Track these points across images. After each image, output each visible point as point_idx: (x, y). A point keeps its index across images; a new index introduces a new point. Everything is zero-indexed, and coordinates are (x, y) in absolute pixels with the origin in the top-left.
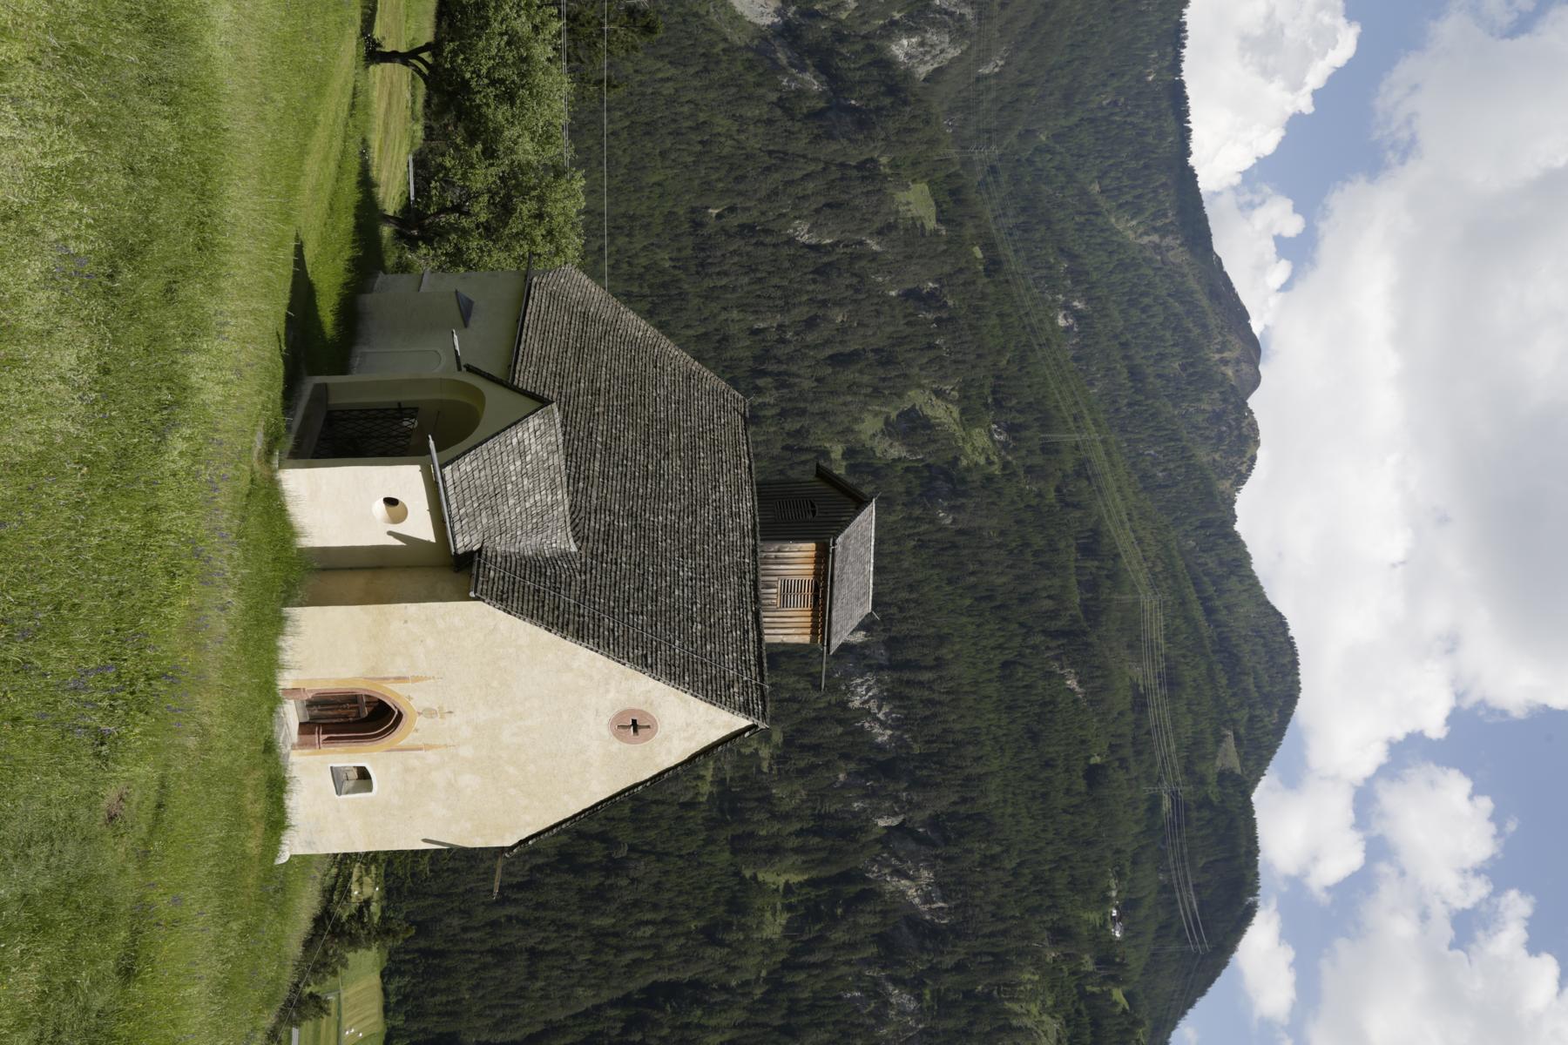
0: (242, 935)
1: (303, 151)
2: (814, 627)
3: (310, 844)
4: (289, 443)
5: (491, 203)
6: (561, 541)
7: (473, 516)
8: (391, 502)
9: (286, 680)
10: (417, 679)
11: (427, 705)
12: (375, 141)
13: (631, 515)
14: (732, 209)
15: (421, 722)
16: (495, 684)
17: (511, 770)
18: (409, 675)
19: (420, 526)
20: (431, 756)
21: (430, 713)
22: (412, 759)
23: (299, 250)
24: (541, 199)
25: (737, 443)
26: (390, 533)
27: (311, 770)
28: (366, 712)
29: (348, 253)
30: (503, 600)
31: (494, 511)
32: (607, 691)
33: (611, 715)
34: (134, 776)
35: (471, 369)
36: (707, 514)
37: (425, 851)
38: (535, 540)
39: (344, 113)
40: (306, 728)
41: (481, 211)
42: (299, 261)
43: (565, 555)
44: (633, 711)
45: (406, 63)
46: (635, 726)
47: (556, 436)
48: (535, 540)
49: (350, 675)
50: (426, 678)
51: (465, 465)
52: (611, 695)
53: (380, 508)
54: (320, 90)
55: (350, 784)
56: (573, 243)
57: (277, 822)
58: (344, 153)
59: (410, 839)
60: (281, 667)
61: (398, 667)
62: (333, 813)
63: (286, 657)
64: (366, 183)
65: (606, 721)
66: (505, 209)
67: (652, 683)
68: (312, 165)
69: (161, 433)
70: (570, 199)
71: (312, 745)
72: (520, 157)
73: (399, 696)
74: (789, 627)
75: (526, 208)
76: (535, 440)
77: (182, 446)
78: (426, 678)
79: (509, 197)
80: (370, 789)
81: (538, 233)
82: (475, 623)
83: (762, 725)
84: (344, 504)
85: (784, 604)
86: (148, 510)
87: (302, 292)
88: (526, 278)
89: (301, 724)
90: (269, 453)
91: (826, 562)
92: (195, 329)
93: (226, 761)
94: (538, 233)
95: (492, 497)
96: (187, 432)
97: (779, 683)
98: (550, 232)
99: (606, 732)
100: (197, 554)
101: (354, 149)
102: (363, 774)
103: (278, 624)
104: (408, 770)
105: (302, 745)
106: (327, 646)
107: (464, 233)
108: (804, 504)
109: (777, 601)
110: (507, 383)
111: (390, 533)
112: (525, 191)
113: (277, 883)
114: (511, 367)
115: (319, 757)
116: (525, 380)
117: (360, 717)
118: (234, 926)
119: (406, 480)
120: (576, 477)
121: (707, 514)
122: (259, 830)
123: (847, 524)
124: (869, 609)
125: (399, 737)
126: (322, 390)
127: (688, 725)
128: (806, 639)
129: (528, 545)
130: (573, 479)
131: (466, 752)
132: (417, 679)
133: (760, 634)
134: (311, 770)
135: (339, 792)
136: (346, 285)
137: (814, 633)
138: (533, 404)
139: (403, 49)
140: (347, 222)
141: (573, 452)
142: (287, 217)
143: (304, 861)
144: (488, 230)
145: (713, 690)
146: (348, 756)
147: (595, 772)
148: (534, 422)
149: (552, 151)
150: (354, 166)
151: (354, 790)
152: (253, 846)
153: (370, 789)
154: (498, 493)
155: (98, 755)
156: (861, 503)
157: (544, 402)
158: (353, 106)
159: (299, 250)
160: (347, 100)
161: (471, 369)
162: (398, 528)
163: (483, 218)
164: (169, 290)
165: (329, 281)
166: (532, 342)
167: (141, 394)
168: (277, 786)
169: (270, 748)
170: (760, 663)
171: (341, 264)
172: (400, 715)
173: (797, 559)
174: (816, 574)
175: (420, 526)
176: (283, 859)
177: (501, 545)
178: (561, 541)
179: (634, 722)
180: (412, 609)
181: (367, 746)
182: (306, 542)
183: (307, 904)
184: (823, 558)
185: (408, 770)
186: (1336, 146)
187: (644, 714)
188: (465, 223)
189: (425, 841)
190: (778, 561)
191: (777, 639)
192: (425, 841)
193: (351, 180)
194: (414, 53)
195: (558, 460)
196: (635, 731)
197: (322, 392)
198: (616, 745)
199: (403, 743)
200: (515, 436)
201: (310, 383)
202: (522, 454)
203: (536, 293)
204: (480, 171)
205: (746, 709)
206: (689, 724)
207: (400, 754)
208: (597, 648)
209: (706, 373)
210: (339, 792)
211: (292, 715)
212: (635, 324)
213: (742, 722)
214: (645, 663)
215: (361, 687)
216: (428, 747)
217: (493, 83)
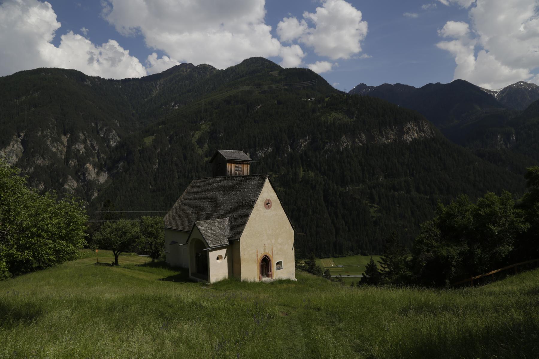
0: (312, 287)
1: (138, 279)
2: (246, 164)
3: (293, 274)
4: (204, 281)
5: (149, 237)
6: (226, 220)
7: (221, 240)
8: (218, 259)
9: (257, 280)
10: (257, 252)
12: (135, 263)
13: (220, 205)
14: (150, 183)
15: (267, 251)
17: (277, 231)
19: (223, 252)
20: (274, 249)
21: (265, 249)
22: (275, 253)
23: (160, 280)
24: (148, 226)
25: (204, 181)
27: (277, 274)
28: (264, 263)
29: (161, 269)
30: (239, 233)
31: (220, 236)
34: (277, 310)
35: (187, 241)
36: (220, 188)
37: (295, 250)
38: (226, 226)
39: (130, 270)
40: (268, 276)
41: (151, 239)
42: (163, 280)
43: (229, 220)
45: (118, 256)
46: (268, 204)
47: (202, 222)
48: (226, 226)
51: (209, 242)
53: (219, 261)
54: (124, 275)
55: (280, 267)
56: (158, 219)
57: (288, 281)
58: (138, 270)
59: (292, 253)
60: (255, 281)
61: (255, 256)
62: (286, 270)
63: (252, 280)
64: (145, 265)
65: (267, 210)
66: (151, 234)
67: (258, 200)
68: (141, 277)
69: (202, 307)
70: (148, 219)
71: (272, 275)
72: (138, 231)
74: (246, 169)
75: (150, 229)
76: (203, 227)
77: (205, 303)
79: (148, 233)
80: (281, 262)
81: (156, 226)
82: (245, 240)
83: (268, 175)
84: (218, 268)
85: (241, 171)
86: (220, 310)
87: (170, 279)
88: (166, 229)
90: (207, 285)
92: (179, 300)
93: (275, 292)
94: (156, 226)
95: (217, 236)
96: (202, 302)
97: (259, 172)
98: (156, 224)
99: (269, 210)
100: (229, 300)
101: (137, 268)
102: (279, 263)
103: (245, 282)
104: (277, 254)
105: (272, 277)
106: (250, 272)
107: (156, 243)
108: (218, 166)
109: (240, 172)
110: (190, 233)
112: (146, 229)
113: (301, 280)
114: (186, 232)
116: (189, 229)
117: (265, 265)
118: (310, 289)
119: (213, 255)
120: (212, 217)
121: (220, 188)
122: (290, 285)
123: (223, 156)
124: (242, 151)
125: (270, 255)
126: (192, 274)
128: (249, 166)
129: (227, 228)
130: (212, 218)
131: (273, 241)
132: (257, 252)
133: (248, 176)
134: (277, 274)
136: (169, 269)
137: (247, 164)
138: (195, 227)
139: (114, 257)
140: (154, 269)
141: (206, 218)
142: (153, 282)
143: (297, 276)
144: (156, 238)
145: (260, 187)
146: (274, 267)
147: (278, 212)
148: (199, 227)
149: (137, 223)
150: (141, 268)
152: (293, 286)
153: (281, 262)
154: (215, 235)
155: (273, 318)
156: (218, 153)
157: (195, 225)
158: (128, 268)
159: (160, 280)
160: (126, 270)
161: (187, 241)
163: (153, 239)
164: (170, 306)
165: (167, 273)
166: (181, 228)
167: (193, 311)
168: (280, 282)
169: (272, 283)
170: (253, 176)
171: (164, 270)
173: (231, 168)
174: (234, 163)
175: (223, 252)
176: (296, 280)
177: (227, 234)
178: (226, 220)
180: (242, 253)
181: (272, 262)
182: (227, 277)
183: (306, 274)
184: (230, 162)
185: (277, 254)
186: (137, 45)
187: (265, 202)
188: (154, 243)
190: (231, 172)
191: (249, 172)
193: (145, 269)
194: (115, 255)
195: (208, 222)
197: (193, 274)
198: (272, 208)
200: (203, 231)
201: (191, 276)
202: (207, 229)
203: (170, 227)
204: (142, 240)
205: (264, 179)
206: (268, 192)
208: (250, 212)
209: (188, 188)
211: (265, 279)
212: (177, 204)
213: (267, 180)
214: (254, 202)
215: (259, 264)
216: (272, 249)
217: (121, 237)
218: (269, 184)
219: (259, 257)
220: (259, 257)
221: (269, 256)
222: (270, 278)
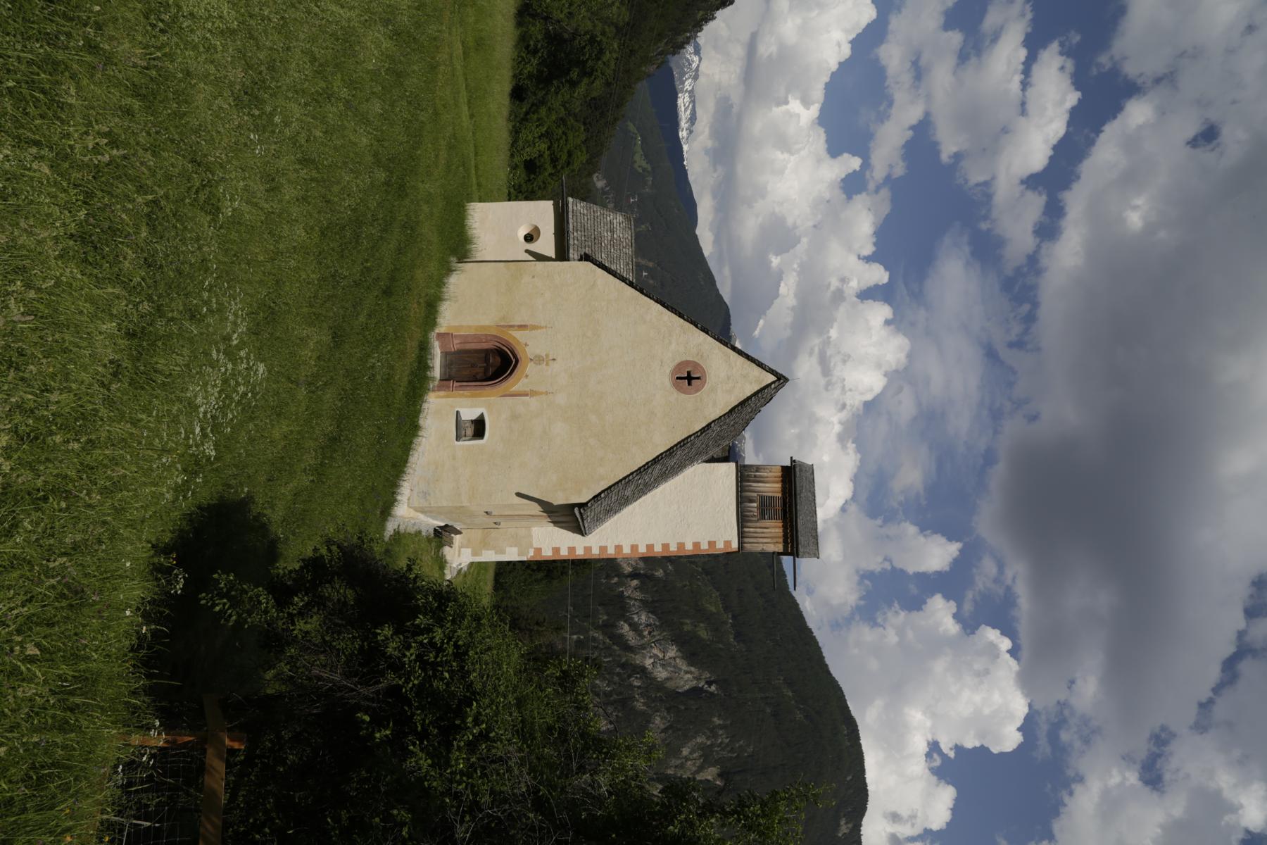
10: (534, 328)
11: (538, 352)
18: (529, 323)
20: (533, 402)
21: (539, 360)
22: (518, 404)
26: (527, 251)
27: (441, 411)
32: (670, 343)
33: (672, 365)
44: (687, 363)
46: (688, 378)
49: (487, 323)
50: (541, 327)
52: (673, 346)
65: (668, 371)
84: (505, 226)
85: (762, 517)
91: (790, 481)
99: (667, 382)
102: (479, 428)
104: (515, 417)
111: (527, 251)
115: (450, 399)
127: (729, 378)
131: (561, 399)
132: (534, 328)
135: (458, 438)
137: (785, 542)
162: (531, 247)
172: (517, 361)
174: (784, 490)
175: (546, 244)
179: (689, 373)
181: (488, 390)
185: (515, 417)
187: (696, 365)
189: (519, 495)
191: (758, 548)
192: (519, 495)
196: (689, 384)
198: (675, 395)
199: (516, 388)
202: (612, 231)
207: (509, 400)
210: (458, 438)
211: (437, 372)
218: (757, 388)
219: (517, 334)
220: (517, 334)
221: (511, 380)
222: (436, 383)
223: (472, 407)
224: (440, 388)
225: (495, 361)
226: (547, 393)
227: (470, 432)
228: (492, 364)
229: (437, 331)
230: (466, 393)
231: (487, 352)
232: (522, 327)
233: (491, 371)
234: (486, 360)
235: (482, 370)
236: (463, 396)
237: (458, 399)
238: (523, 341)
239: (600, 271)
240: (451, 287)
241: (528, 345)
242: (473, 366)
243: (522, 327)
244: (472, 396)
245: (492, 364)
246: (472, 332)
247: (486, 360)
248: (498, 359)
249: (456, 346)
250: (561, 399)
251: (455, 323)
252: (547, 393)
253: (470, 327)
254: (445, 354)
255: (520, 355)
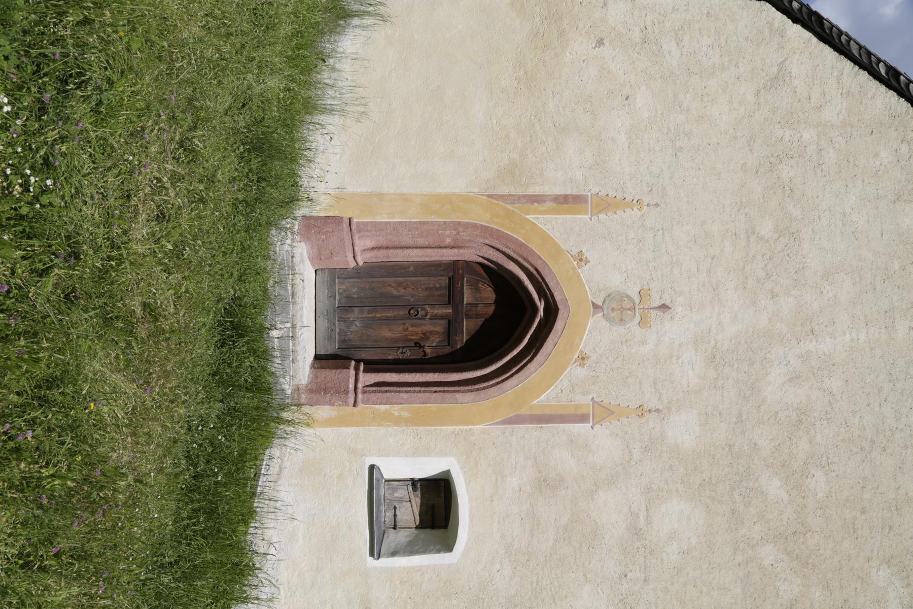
10: (605, 205)
11: (616, 281)
16: (766, 228)
17: (775, 488)
18: (591, 189)
20: (603, 441)
50: (623, 204)
55: (401, 537)
73: (558, 251)
78: (623, 204)
80: (448, 546)
89: (317, 357)
104: (546, 484)
131: (683, 430)
132: (605, 205)
151: (411, 549)
172: (552, 311)
181: (465, 402)
185: (546, 484)
199: (548, 398)
223: (416, 453)
224: (319, 392)
225: (480, 298)
226: (642, 412)
227: (409, 511)
228: (478, 319)
229: (301, 211)
230: (396, 410)
231: (455, 273)
232: (568, 202)
233: (467, 328)
234: (452, 295)
235: (440, 327)
236: (387, 419)
237: (375, 431)
238: (570, 245)
239: (797, 31)
240: (345, 66)
241: (584, 261)
242: (412, 311)
243: (568, 202)
244: (416, 421)
245: (478, 319)
246: (413, 215)
247: (452, 295)
248: (489, 294)
249: (362, 253)
250: (683, 430)
251: (354, 187)
252: (642, 412)
253: (405, 198)
254: (330, 276)
255: (563, 292)
